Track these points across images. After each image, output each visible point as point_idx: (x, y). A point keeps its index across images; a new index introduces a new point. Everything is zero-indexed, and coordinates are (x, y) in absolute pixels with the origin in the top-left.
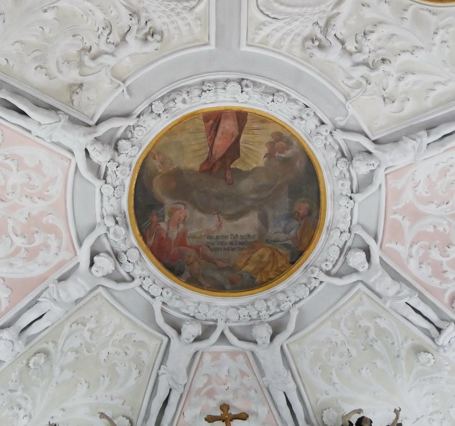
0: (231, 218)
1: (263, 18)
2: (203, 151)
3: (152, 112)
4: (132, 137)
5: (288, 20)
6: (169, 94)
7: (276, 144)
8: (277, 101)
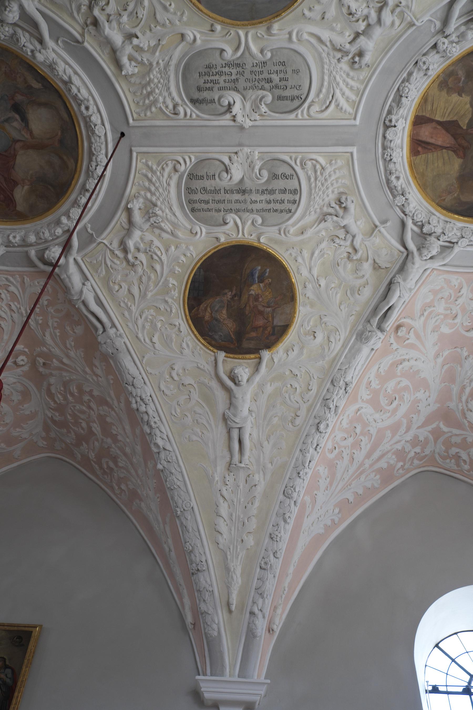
1: (333, 106)
2: (446, 155)
3: (403, 205)
4: (422, 221)
5: (334, 85)
6: (391, 189)
7: (450, 86)
8: (407, 93)
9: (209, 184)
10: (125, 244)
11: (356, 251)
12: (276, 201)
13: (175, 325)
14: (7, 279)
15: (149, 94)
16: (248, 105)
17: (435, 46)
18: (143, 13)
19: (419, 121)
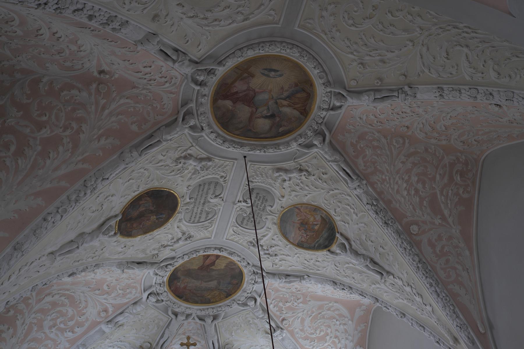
0: (206, 282)
9: (211, 191)
10: (190, 159)
11: (164, 247)
12: (196, 216)
13: (138, 188)
14: (175, 83)
15: (262, 175)
16: (245, 208)
17: (249, 263)
18: (298, 188)
19: (218, 257)
